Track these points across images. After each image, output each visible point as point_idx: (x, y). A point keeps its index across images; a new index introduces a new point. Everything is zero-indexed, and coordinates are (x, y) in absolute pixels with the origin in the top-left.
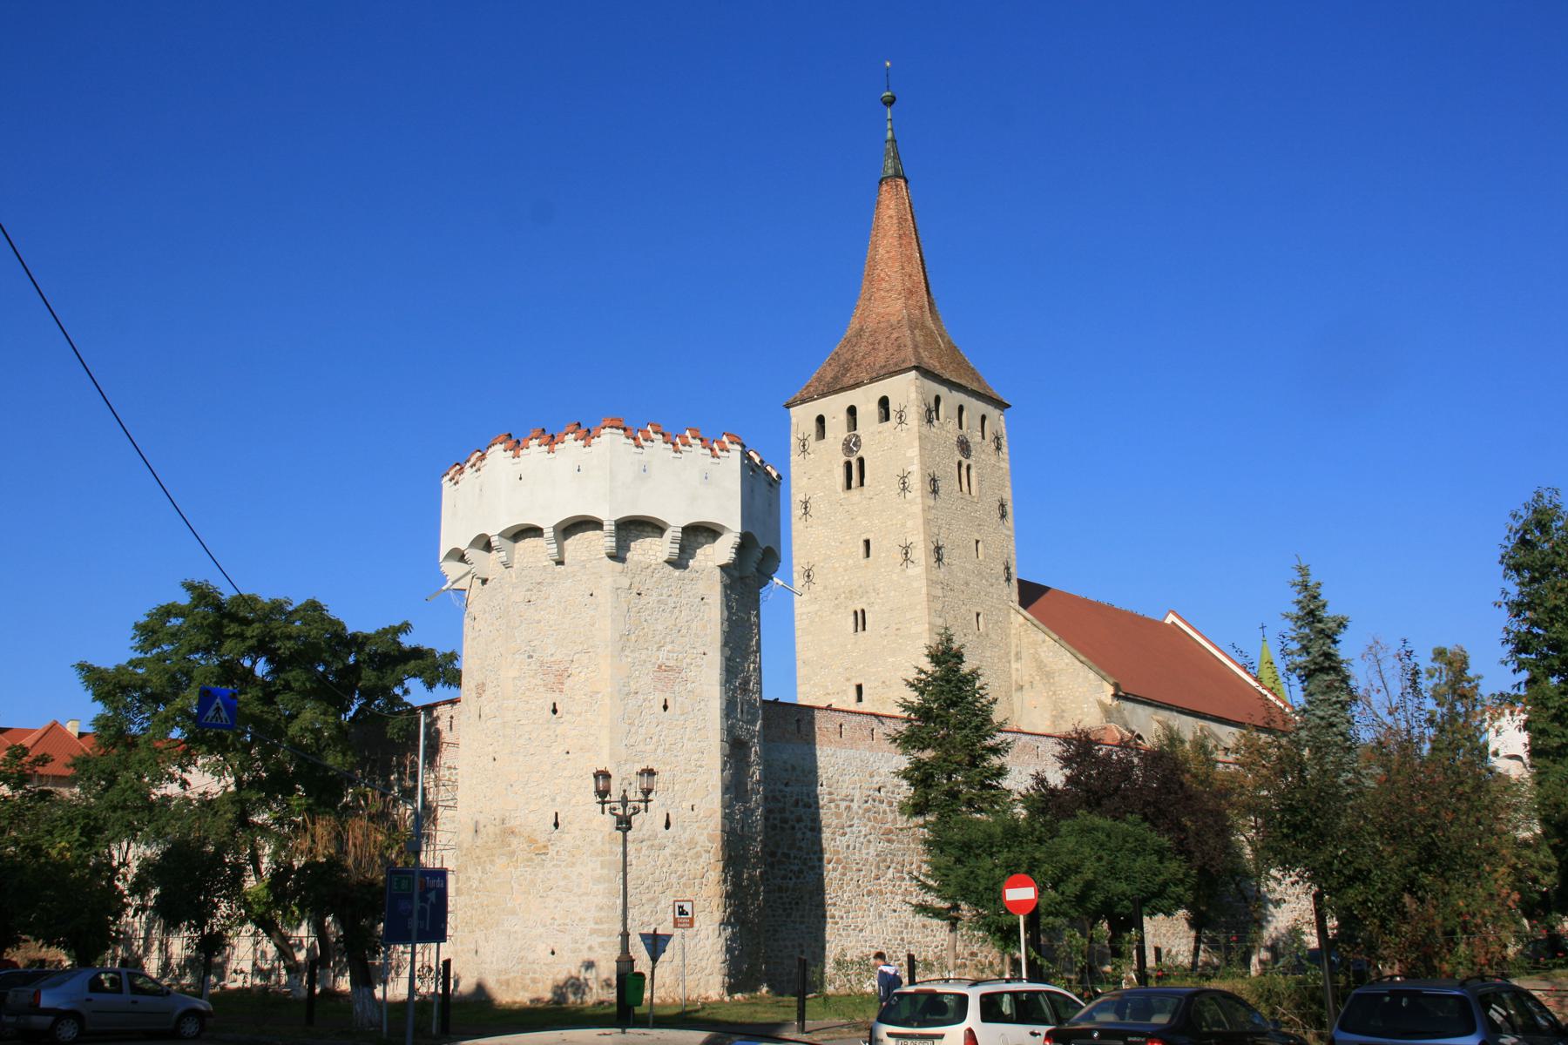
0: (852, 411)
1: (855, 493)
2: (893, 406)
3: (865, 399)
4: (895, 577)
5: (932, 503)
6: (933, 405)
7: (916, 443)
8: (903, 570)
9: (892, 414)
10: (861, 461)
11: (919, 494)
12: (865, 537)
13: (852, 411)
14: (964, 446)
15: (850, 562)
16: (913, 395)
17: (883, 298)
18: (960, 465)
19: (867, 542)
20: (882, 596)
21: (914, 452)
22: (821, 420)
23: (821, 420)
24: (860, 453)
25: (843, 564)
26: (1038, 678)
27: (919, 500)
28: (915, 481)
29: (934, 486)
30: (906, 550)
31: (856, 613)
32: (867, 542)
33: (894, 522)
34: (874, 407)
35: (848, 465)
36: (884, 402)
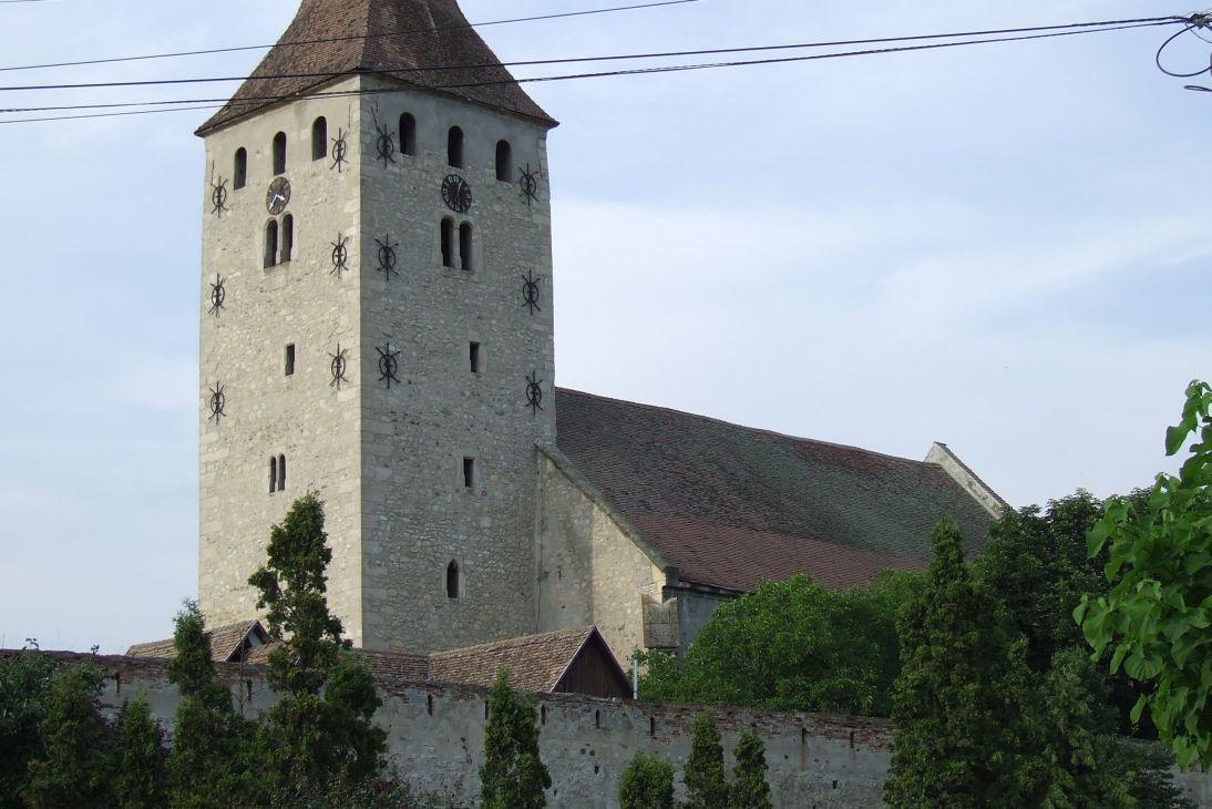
0: (280, 140)
1: (280, 275)
3: (295, 122)
4: (322, 402)
5: (382, 286)
6: (393, 125)
7: (357, 192)
8: (333, 393)
9: (330, 145)
10: (289, 220)
11: (357, 270)
12: (288, 342)
13: (280, 140)
14: (457, 195)
15: (270, 380)
16: (356, 116)
18: (446, 225)
19: (291, 350)
20: (306, 433)
21: (353, 206)
22: (241, 155)
23: (241, 155)
24: (288, 209)
26: (568, 560)
27: (357, 283)
28: (353, 251)
29: (383, 257)
30: (338, 359)
31: (273, 461)
32: (291, 350)
34: (307, 134)
35: (272, 227)
36: (320, 125)
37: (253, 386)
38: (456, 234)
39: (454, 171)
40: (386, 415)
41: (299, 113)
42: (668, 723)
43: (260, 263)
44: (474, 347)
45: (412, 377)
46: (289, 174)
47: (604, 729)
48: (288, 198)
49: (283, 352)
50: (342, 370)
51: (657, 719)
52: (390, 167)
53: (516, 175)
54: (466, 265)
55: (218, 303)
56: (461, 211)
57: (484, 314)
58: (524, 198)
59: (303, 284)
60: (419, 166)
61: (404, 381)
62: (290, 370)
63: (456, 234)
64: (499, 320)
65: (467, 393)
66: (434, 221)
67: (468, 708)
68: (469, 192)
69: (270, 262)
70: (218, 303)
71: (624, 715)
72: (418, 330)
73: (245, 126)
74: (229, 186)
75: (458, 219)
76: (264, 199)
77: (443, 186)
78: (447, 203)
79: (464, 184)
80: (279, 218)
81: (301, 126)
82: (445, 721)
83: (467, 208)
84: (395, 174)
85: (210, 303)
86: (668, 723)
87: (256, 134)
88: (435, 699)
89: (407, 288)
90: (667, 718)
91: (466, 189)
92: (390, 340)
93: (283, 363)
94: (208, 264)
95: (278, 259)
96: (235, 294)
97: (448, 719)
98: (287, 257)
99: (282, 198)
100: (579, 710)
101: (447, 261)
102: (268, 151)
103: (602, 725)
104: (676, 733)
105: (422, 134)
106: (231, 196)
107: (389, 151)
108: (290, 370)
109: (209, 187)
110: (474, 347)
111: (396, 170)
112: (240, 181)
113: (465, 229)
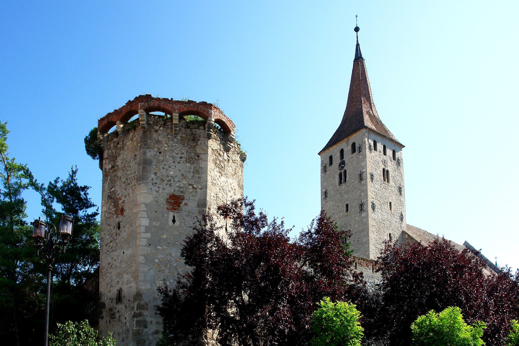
0: (342, 151)
1: (343, 186)
2: (357, 146)
4: (357, 218)
9: (357, 149)
10: (345, 172)
12: (346, 203)
13: (342, 151)
15: (341, 214)
17: (355, 105)
19: (347, 205)
22: (331, 157)
23: (331, 157)
24: (345, 168)
25: (339, 216)
32: (347, 205)
33: (357, 195)
34: (350, 147)
35: (340, 175)
36: (354, 145)
37: (336, 217)
41: (347, 142)
43: (337, 184)
46: (345, 159)
48: (345, 165)
49: (345, 206)
50: (362, 208)
55: (326, 196)
59: (350, 187)
62: (347, 210)
69: (340, 183)
70: (326, 196)
73: (331, 149)
74: (328, 166)
76: (338, 167)
80: (343, 171)
81: (348, 146)
85: (323, 197)
87: (335, 151)
93: (345, 209)
95: (342, 182)
96: (331, 193)
98: (345, 181)
99: (343, 166)
102: (338, 154)
106: (328, 167)
108: (347, 210)
109: (322, 167)
112: (331, 163)
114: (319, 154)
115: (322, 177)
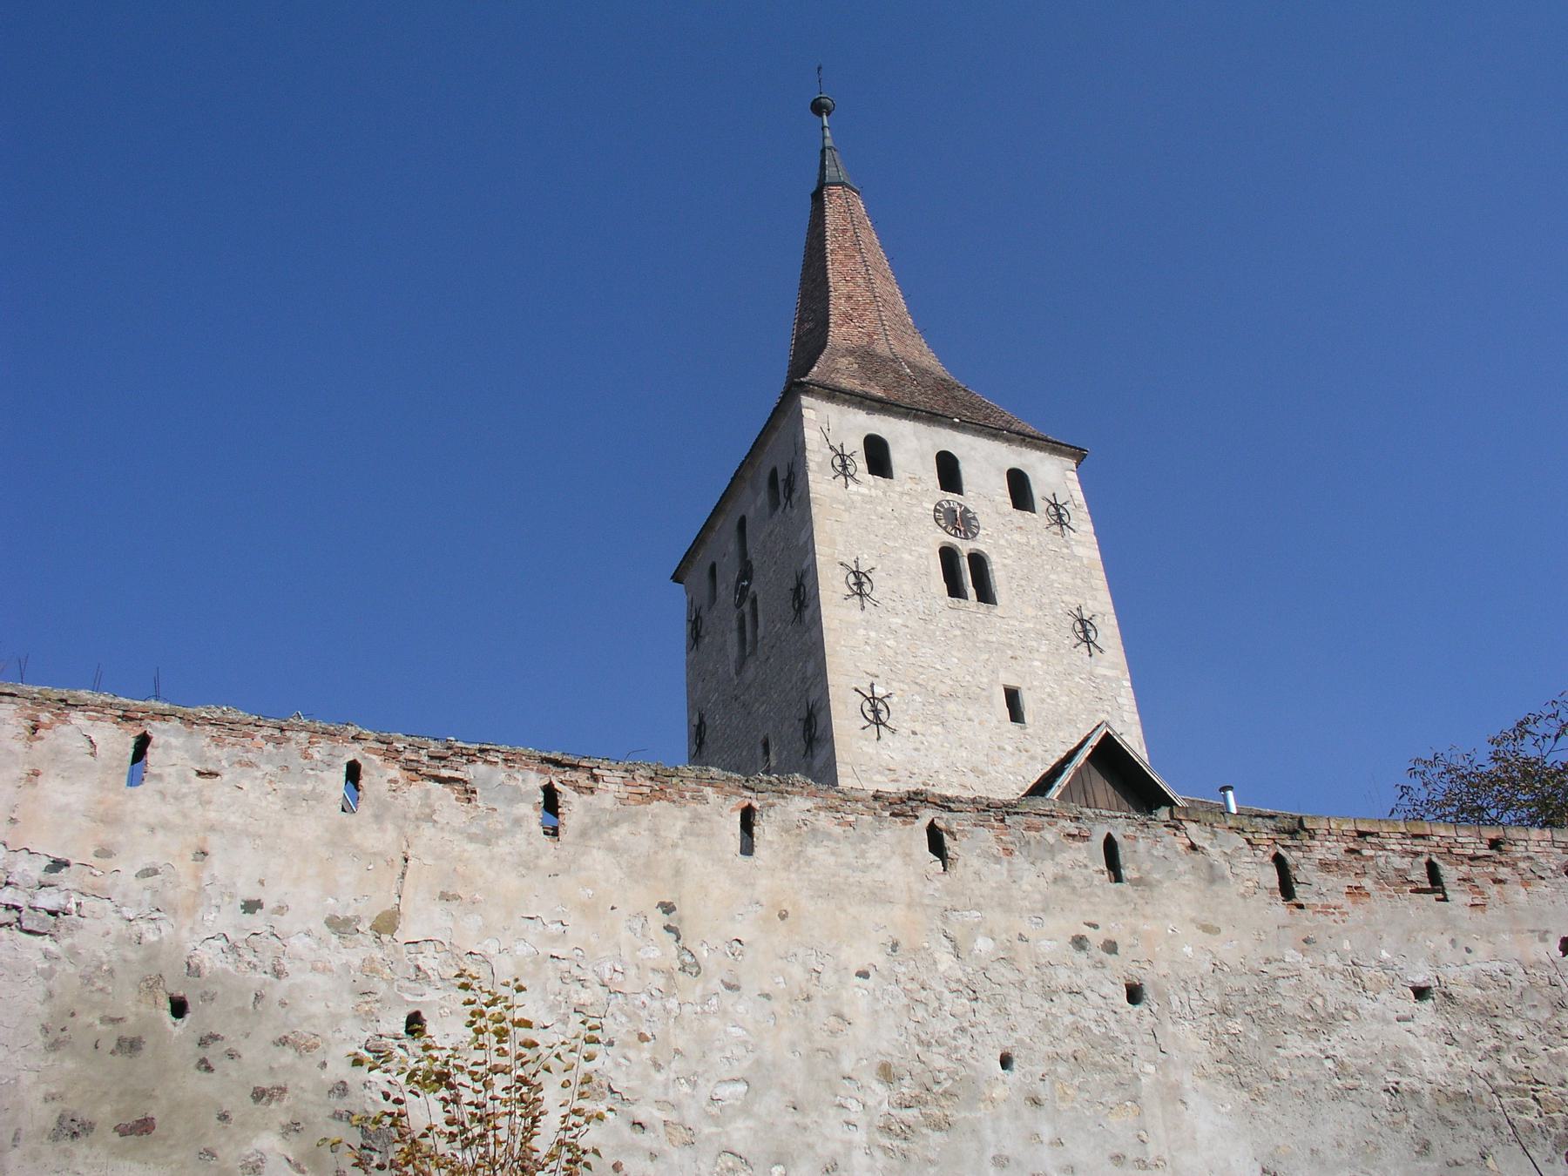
2: (782, 475)
6: (855, 446)
18: (948, 556)
38: (965, 564)
39: (950, 496)
40: (879, 772)
42: (1324, 866)
43: (733, 671)
44: (1012, 697)
45: (918, 727)
47: (1138, 882)
51: (1292, 857)
52: (852, 486)
53: (1040, 505)
54: (986, 595)
56: (966, 538)
57: (1019, 653)
58: (1056, 528)
60: (898, 489)
61: (904, 731)
63: (965, 564)
64: (1043, 662)
65: (1009, 749)
66: (927, 546)
67: (680, 824)
68: (974, 518)
71: (1193, 847)
72: (920, 670)
75: (964, 547)
77: (936, 510)
78: (945, 528)
79: (967, 510)
80: (747, 607)
82: (598, 855)
83: (975, 535)
84: (863, 495)
86: (1324, 866)
88: (567, 795)
89: (895, 620)
90: (1319, 853)
91: (970, 515)
92: (875, 680)
94: (692, 706)
97: (612, 849)
100: (1050, 836)
101: (955, 590)
103: (1126, 873)
104: (1356, 892)
105: (897, 457)
107: (851, 470)
110: (1012, 697)
111: (863, 490)
113: (978, 561)
114: (677, 578)
115: (690, 665)
